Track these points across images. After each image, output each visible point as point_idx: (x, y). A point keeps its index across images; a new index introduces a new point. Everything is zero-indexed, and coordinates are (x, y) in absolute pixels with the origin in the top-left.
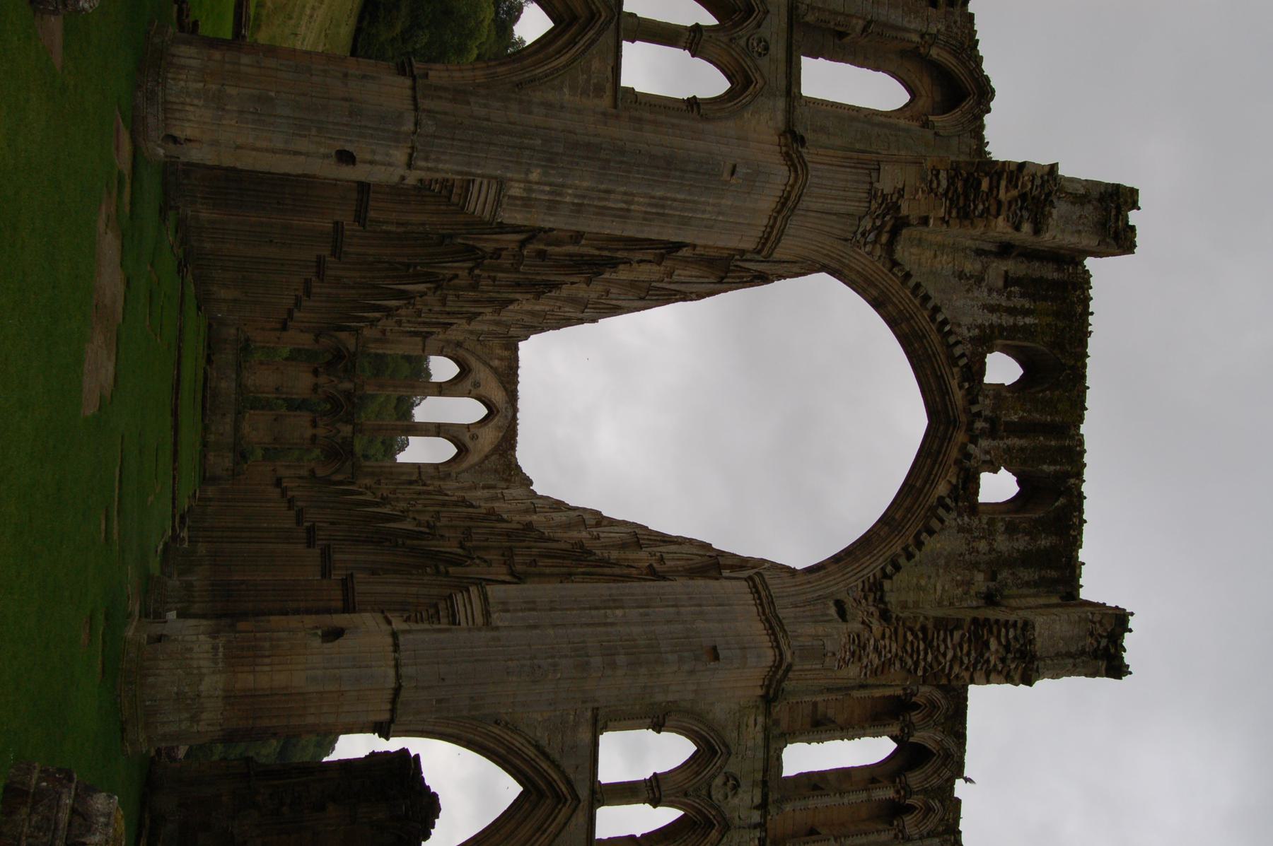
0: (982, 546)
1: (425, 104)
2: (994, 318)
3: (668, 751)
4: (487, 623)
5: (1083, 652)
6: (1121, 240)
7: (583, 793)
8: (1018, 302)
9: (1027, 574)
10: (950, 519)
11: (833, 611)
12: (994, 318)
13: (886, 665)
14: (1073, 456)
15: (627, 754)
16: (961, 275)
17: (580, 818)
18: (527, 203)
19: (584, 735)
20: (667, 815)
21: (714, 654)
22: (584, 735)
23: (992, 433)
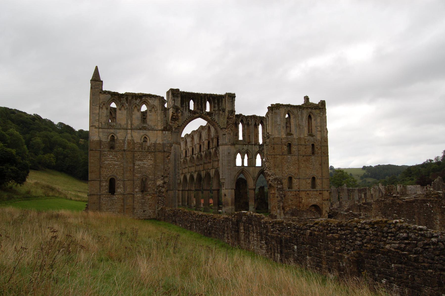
0: (217, 112)
1: (171, 189)
2: (187, 109)
3: (239, 156)
4: (225, 179)
5: (232, 102)
6: (178, 90)
7: (242, 168)
8: (185, 105)
9: (220, 105)
10: (213, 117)
11: (224, 136)
12: (187, 109)
13: (231, 130)
14: (206, 95)
15: (239, 163)
16: (182, 115)
17: (245, 168)
19: (236, 168)
20: (246, 156)
21: (229, 153)
22: (236, 168)
23: (202, 110)
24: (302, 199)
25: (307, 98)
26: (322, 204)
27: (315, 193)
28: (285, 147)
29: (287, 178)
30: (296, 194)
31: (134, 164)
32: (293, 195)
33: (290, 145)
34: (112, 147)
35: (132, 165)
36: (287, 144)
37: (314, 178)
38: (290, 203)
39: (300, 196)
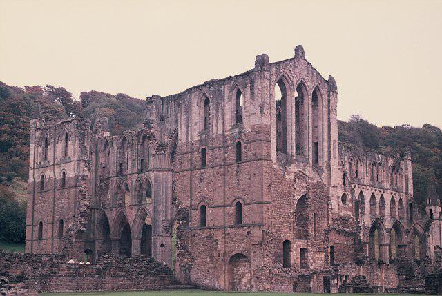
18: (166, 216)
24: (217, 244)
25: (299, 49)
26: (250, 253)
27: (240, 230)
28: (198, 155)
29: (199, 208)
30: (210, 235)
31: (55, 204)
32: (207, 237)
33: (204, 152)
34: (42, 188)
35: (52, 206)
36: (200, 151)
37: (239, 206)
38: (202, 249)
39: (215, 238)
